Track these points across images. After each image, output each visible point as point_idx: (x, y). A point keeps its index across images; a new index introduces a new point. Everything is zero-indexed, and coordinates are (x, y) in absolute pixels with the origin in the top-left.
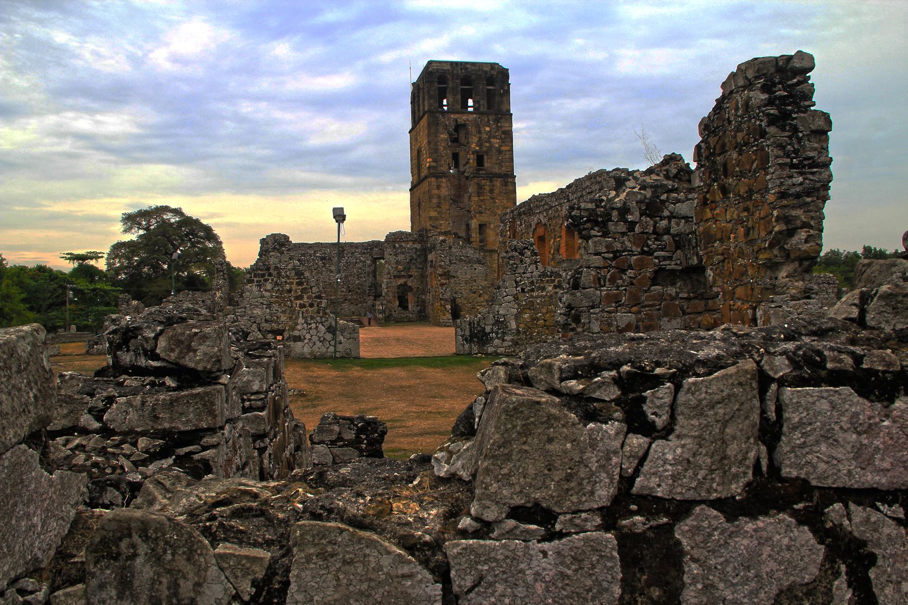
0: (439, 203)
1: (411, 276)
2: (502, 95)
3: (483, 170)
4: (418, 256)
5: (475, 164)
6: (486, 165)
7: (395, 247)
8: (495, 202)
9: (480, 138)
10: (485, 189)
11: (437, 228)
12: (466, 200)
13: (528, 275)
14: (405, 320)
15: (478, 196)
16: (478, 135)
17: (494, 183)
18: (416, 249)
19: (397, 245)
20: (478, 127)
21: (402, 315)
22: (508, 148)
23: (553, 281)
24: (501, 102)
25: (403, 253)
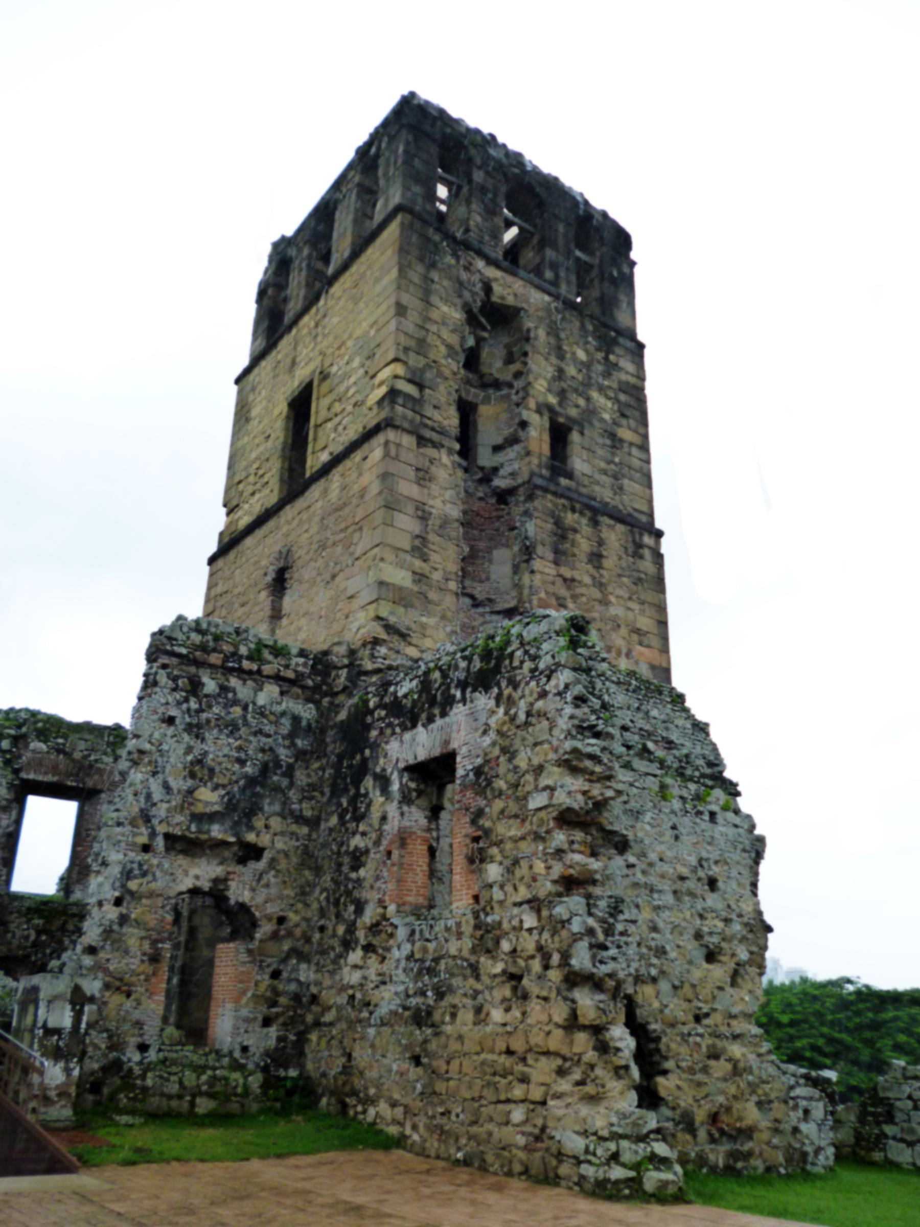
0: (422, 538)
1: (250, 853)
2: (614, 282)
4: (301, 755)
7: (195, 686)
8: (605, 602)
10: (573, 543)
11: (403, 636)
14: (204, 1105)
15: (556, 563)
16: (553, 359)
18: (296, 719)
19: (210, 685)
20: (553, 331)
21: (190, 1078)
25: (233, 728)
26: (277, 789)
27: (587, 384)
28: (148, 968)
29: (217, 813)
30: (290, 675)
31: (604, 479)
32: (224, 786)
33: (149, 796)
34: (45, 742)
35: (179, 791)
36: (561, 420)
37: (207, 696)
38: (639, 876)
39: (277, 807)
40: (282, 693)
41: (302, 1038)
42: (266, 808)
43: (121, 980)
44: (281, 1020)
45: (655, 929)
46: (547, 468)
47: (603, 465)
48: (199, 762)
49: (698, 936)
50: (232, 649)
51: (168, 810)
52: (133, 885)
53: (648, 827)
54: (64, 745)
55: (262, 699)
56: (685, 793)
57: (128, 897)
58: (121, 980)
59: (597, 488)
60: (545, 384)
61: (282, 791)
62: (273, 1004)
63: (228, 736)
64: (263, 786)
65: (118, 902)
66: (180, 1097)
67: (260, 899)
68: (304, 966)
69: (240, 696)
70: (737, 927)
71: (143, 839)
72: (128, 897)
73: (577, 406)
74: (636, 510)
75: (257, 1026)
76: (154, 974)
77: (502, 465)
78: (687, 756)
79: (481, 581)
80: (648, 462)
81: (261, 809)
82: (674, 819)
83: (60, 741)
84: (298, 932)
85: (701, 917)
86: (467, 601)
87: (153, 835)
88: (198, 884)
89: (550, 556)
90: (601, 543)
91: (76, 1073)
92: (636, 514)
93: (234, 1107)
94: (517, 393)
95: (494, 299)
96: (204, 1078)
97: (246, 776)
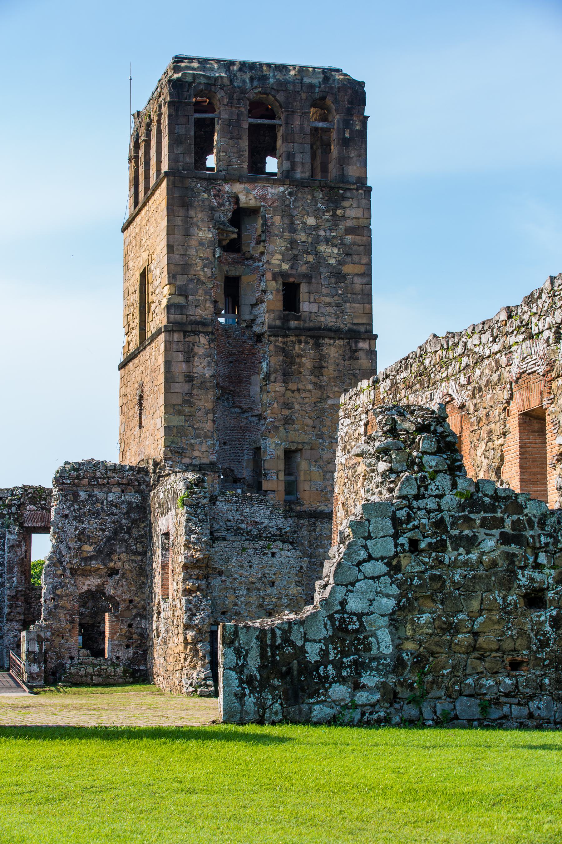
1: (113, 572)
3: (298, 318)
5: (279, 305)
6: (305, 307)
7: (76, 496)
9: (293, 242)
10: (300, 364)
12: (255, 389)
13: (431, 504)
15: (285, 382)
16: (287, 235)
17: (325, 350)
18: (130, 504)
19: (83, 495)
21: (90, 670)
22: (359, 269)
23: (500, 523)
24: (343, 161)
25: (96, 514)
26: (123, 540)
27: (317, 241)
28: (69, 626)
29: (93, 555)
30: (125, 481)
31: (330, 310)
32: (96, 543)
33: (60, 553)
34: (34, 505)
35: (74, 548)
36: (291, 280)
37: (82, 501)
38: (228, 584)
39: (123, 549)
40: (123, 491)
41: (145, 652)
42: (118, 550)
43: (59, 631)
44: (134, 645)
45: (236, 605)
46: (280, 318)
47: (328, 300)
48: (82, 533)
49: (261, 606)
50: (92, 475)
51: (70, 558)
52: (58, 592)
53: (234, 564)
54: (45, 504)
55: (111, 497)
56: (257, 546)
57: (57, 597)
58: (59, 631)
59: (322, 319)
60: (280, 257)
61: (126, 541)
62: (131, 638)
63: (95, 519)
64: (115, 540)
65: (53, 599)
66: (86, 676)
67: (119, 592)
68: (143, 621)
69: (99, 498)
70: (285, 601)
71: (60, 572)
72: (57, 597)
73: (307, 263)
74: (355, 324)
75: (123, 648)
76: (73, 628)
77: (256, 316)
78: (265, 527)
79: (245, 397)
80: (370, 283)
81: (115, 551)
82: (249, 559)
83: (42, 502)
84: (140, 606)
85: (263, 598)
86: (238, 410)
87: (64, 569)
88: (90, 588)
89: (280, 378)
90: (322, 358)
91: (43, 668)
92: (355, 327)
93: (111, 681)
94: (263, 266)
95: (241, 205)
96: (96, 669)
97: (106, 536)
